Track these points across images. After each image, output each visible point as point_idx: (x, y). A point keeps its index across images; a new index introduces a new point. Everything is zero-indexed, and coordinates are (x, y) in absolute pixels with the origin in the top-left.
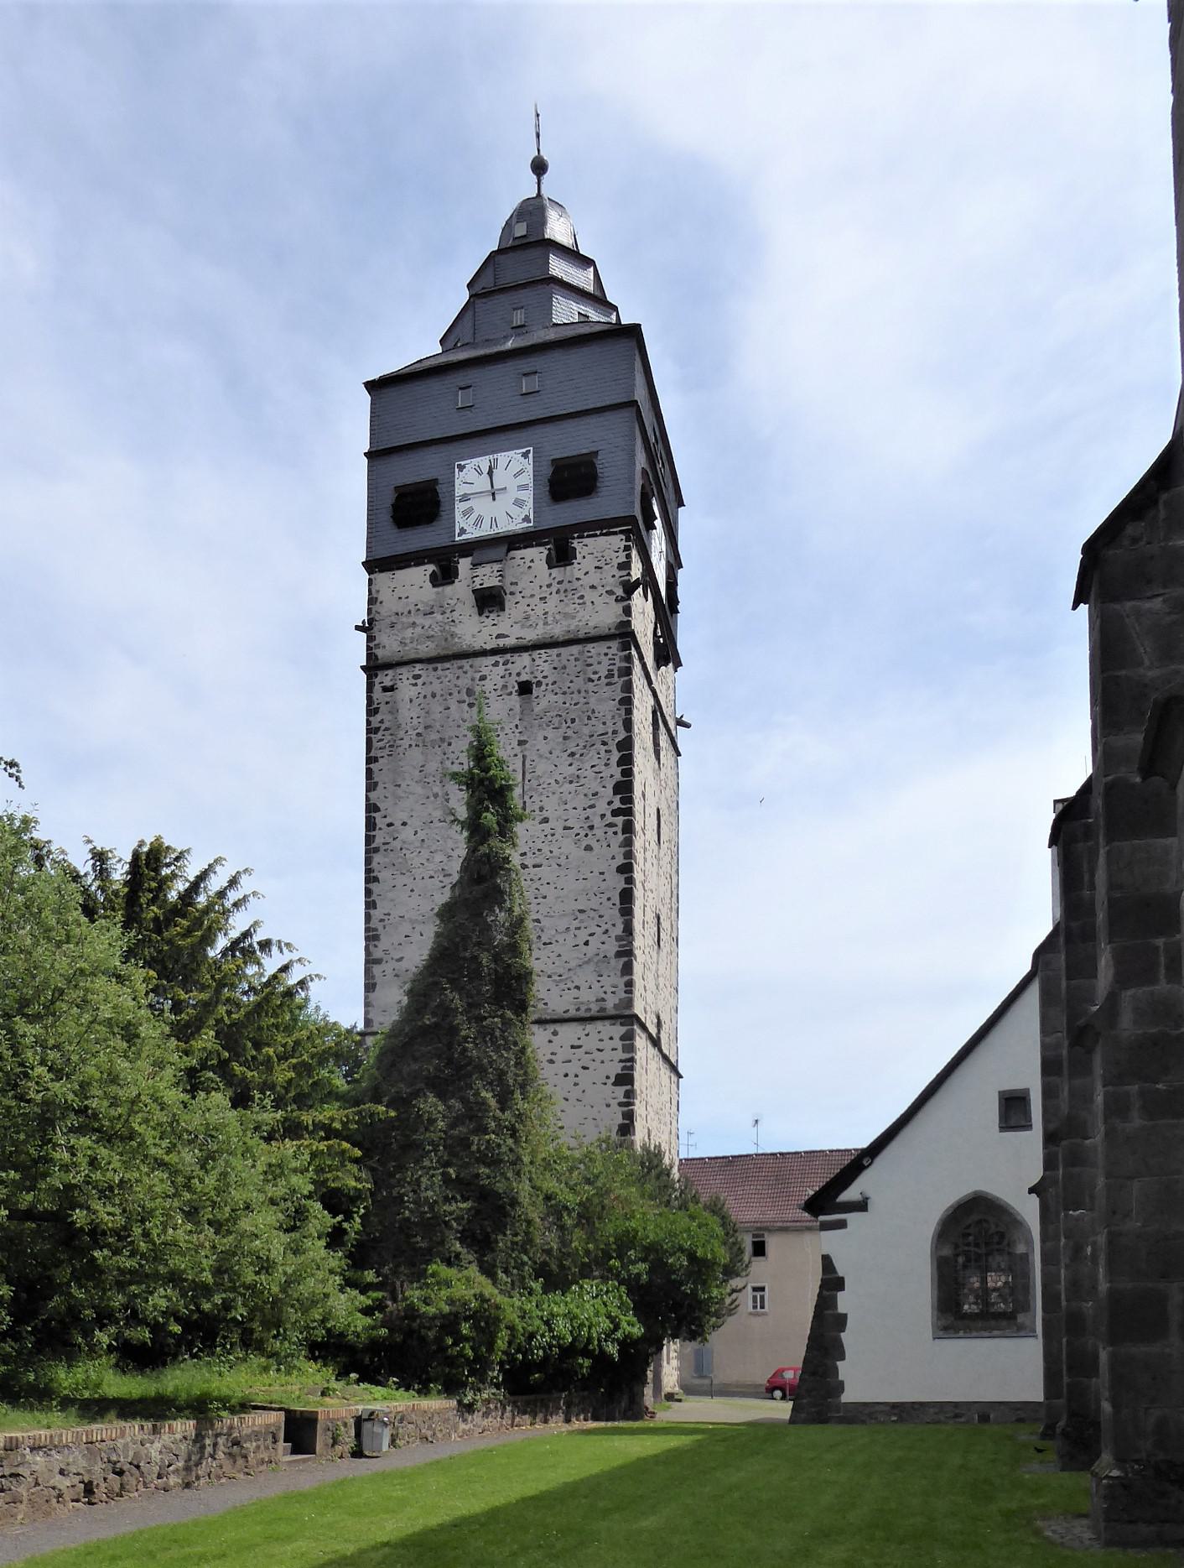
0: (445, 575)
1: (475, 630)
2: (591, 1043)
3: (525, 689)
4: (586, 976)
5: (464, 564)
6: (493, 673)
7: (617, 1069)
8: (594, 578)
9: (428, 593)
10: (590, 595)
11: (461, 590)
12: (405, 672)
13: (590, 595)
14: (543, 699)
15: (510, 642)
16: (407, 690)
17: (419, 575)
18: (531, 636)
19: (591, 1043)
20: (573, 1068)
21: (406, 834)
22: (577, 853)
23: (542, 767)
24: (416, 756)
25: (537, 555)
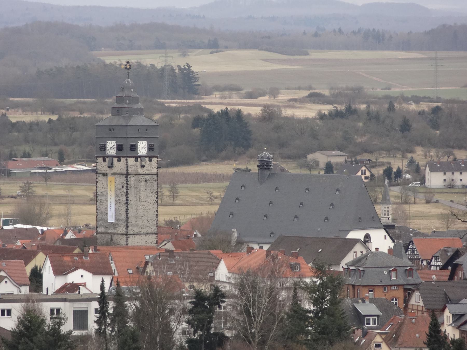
0: (136, 160)
1: (140, 171)
2: (153, 237)
3: (146, 181)
4: (152, 227)
5: (139, 159)
6: (143, 178)
7: (156, 242)
8: (154, 165)
9: (134, 163)
10: (154, 167)
11: (139, 163)
12: (132, 176)
13: (154, 167)
14: (148, 183)
15: (144, 173)
16: (132, 179)
17: (133, 159)
18: (147, 172)
19: (153, 237)
20: (151, 241)
21: (132, 202)
22: (152, 207)
23: (148, 194)
24: (133, 189)
25: (147, 159)
